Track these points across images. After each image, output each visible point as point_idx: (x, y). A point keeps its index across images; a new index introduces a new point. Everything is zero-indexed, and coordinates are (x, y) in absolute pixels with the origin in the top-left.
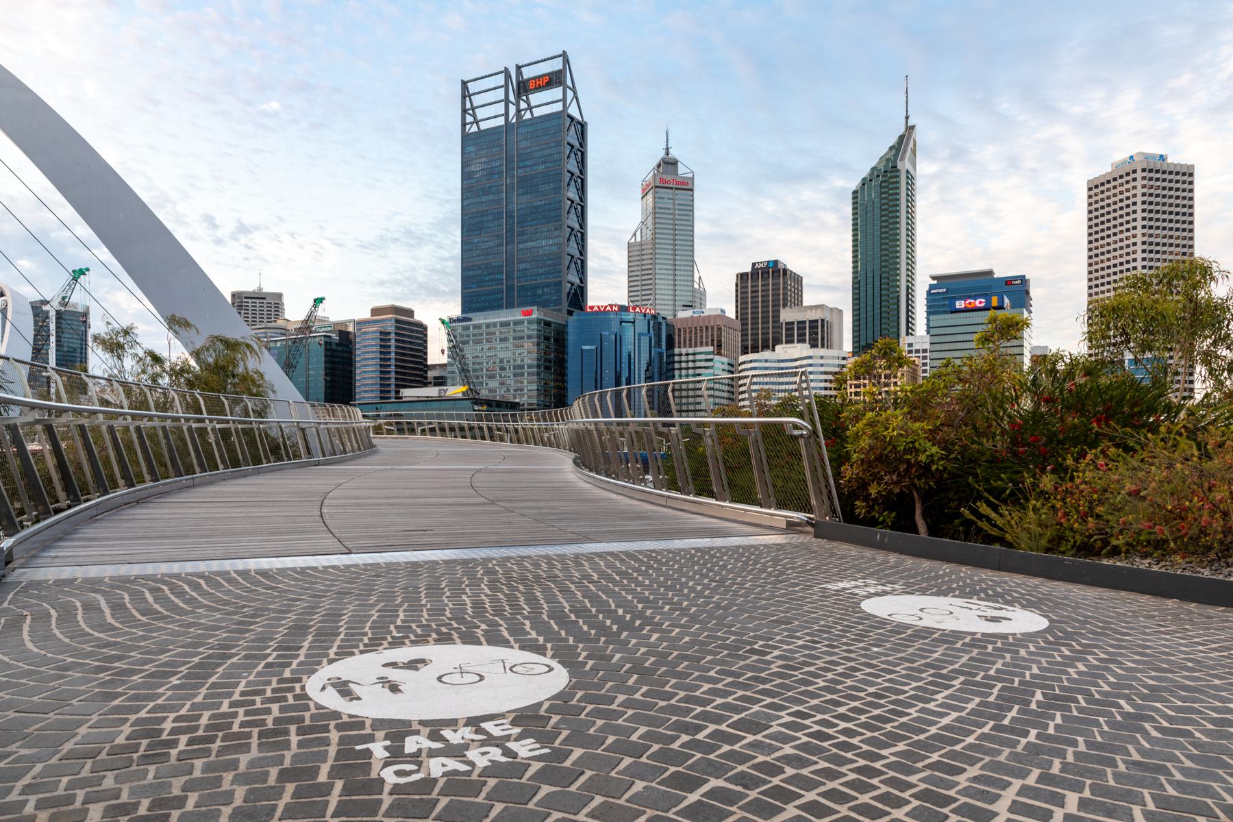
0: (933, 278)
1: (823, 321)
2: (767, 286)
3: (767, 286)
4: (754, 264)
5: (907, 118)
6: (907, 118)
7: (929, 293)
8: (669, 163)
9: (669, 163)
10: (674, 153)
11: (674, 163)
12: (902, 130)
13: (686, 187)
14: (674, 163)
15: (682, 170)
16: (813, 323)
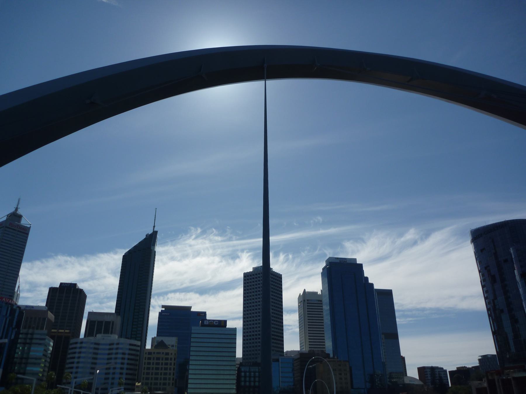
0: (163, 306)
1: (113, 322)
2: (67, 297)
3: (67, 297)
4: (61, 284)
5: (154, 227)
6: (154, 227)
7: (160, 314)
8: (15, 217)
9: (15, 217)
10: (20, 212)
11: (20, 217)
12: (150, 232)
13: (25, 231)
14: (20, 217)
15: (23, 222)
16: (108, 323)
